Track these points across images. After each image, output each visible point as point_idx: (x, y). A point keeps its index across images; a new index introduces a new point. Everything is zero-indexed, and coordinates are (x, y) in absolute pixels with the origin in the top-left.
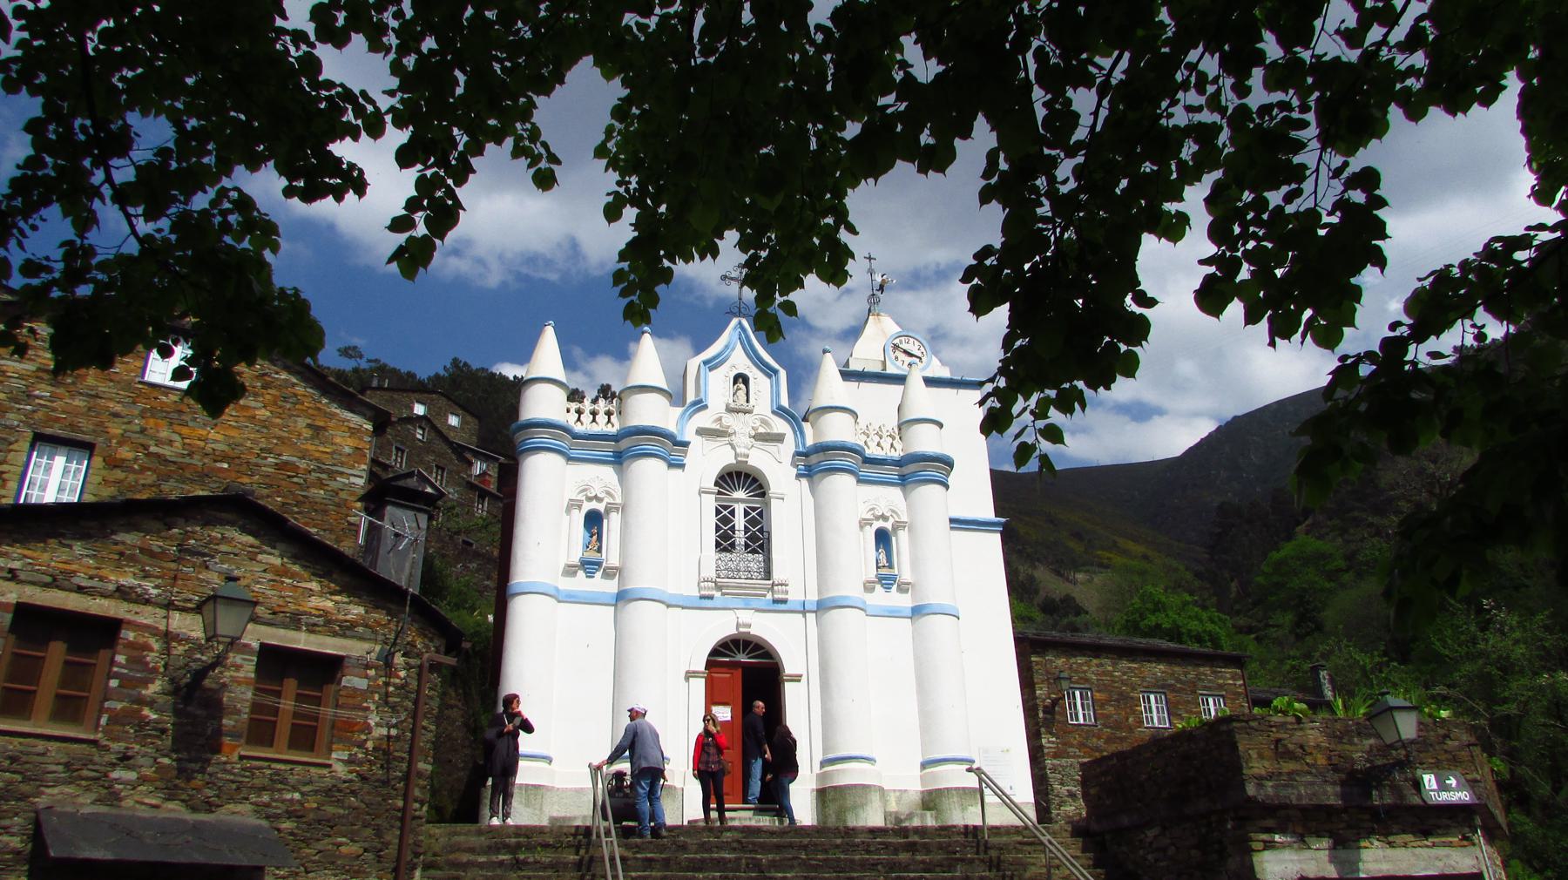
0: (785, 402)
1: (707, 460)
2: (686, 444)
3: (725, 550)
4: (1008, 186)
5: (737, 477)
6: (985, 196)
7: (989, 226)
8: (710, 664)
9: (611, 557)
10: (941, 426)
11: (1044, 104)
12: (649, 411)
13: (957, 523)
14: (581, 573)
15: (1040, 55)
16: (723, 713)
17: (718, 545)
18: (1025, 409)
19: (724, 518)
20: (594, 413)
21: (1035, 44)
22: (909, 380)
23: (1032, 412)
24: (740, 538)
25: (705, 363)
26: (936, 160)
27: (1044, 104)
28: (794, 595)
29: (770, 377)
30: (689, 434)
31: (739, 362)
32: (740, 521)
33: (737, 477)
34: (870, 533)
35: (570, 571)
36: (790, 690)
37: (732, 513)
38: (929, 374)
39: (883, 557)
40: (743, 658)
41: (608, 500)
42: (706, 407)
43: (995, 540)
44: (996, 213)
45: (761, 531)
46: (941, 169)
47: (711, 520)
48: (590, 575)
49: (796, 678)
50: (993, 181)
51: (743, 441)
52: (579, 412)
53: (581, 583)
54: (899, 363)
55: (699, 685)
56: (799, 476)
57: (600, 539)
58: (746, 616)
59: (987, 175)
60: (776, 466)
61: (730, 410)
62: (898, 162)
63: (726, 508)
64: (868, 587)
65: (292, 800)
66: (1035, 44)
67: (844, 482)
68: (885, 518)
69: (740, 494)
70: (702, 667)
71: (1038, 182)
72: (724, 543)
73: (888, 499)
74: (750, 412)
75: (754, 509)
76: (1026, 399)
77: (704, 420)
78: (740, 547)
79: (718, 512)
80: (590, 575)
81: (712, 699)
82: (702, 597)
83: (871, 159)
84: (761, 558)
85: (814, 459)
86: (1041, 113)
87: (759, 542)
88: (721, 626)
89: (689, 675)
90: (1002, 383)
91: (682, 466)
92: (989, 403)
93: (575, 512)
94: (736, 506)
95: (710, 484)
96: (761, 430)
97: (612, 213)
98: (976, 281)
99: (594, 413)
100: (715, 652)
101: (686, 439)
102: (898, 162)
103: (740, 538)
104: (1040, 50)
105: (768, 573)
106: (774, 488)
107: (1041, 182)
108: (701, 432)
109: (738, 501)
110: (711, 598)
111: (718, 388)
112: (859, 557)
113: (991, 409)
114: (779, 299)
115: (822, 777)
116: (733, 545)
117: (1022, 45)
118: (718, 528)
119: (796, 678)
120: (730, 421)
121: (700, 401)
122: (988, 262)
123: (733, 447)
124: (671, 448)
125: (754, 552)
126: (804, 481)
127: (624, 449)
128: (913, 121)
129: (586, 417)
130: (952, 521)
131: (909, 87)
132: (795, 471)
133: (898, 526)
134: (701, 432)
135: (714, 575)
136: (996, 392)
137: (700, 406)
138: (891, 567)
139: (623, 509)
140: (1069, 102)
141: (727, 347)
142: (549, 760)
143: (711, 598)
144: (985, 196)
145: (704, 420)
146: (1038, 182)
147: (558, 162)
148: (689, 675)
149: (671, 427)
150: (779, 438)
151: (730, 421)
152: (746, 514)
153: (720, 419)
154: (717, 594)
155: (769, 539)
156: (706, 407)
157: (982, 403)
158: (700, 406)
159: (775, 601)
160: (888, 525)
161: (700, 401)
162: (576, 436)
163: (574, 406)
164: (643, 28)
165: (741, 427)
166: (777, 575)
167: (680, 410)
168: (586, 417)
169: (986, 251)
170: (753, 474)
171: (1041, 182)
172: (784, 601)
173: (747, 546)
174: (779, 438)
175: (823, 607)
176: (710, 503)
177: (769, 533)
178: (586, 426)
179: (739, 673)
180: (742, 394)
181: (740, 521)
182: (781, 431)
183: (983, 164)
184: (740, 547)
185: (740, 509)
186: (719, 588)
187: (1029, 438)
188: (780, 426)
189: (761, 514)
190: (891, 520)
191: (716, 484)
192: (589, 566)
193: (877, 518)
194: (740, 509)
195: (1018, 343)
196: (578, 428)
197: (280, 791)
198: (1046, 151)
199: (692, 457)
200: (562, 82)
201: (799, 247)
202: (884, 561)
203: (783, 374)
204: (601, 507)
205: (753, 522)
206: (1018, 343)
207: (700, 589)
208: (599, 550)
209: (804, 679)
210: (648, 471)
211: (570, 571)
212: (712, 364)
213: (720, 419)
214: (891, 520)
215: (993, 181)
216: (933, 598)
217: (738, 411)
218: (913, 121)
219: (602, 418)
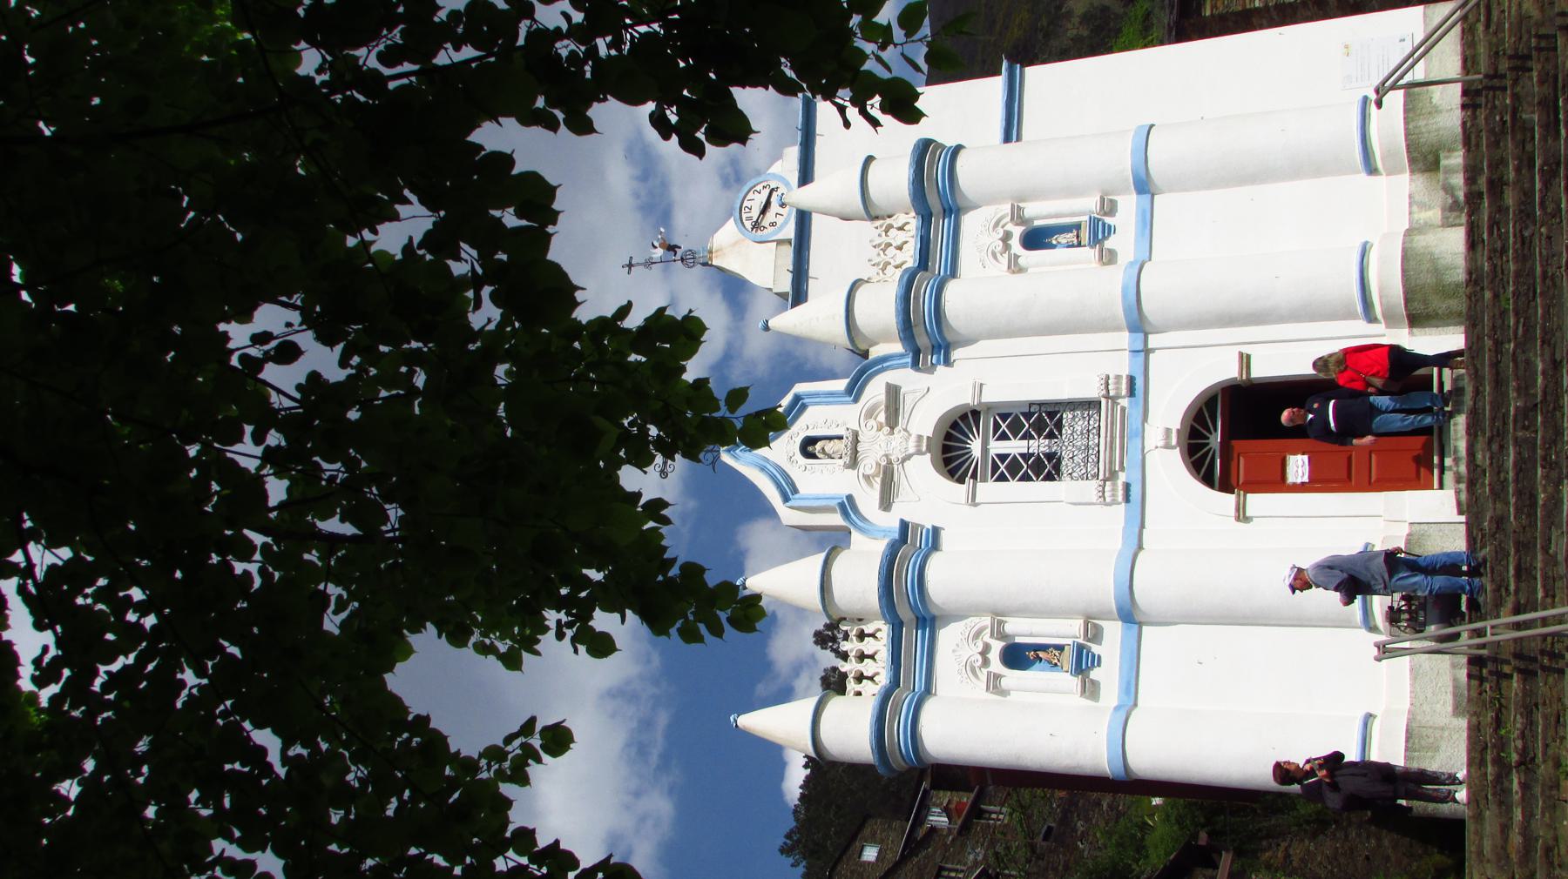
0: (840, 385)
1: (927, 495)
2: (904, 526)
3: (1057, 467)
4: (567, 97)
5: (950, 452)
6: (583, 126)
7: (622, 121)
8: (1226, 487)
9: (1068, 631)
11: (457, 49)
12: (858, 578)
13: (1011, 130)
14: (1095, 674)
15: (387, 58)
16: (1298, 467)
17: (1049, 478)
18: (879, 59)
19: (1011, 469)
20: (862, 657)
21: (373, 63)
22: (805, 205)
23: (883, 47)
24: (1039, 446)
25: (786, 499)
26: (537, 198)
27: (457, 49)
28: (1122, 366)
29: (804, 407)
30: (889, 522)
31: (782, 450)
32: (1015, 447)
33: (950, 452)
34: (1029, 257)
35: (1091, 690)
36: (1260, 371)
37: (1003, 457)
38: (794, 177)
39: (1063, 239)
40: (1216, 439)
41: (986, 637)
42: (850, 498)
43: (1037, 77)
44: (608, 113)
45: (1028, 416)
46: (550, 191)
47: (1014, 487)
48: (1096, 661)
49: (1245, 360)
50: (560, 116)
51: (897, 444)
52: (860, 678)
53: (1108, 674)
54: (780, 220)
55: (1257, 502)
56: (947, 362)
57: (1044, 648)
58: (1154, 435)
59: (552, 126)
60: (935, 395)
61: (854, 463)
62: (551, 256)
63: (995, 467)
64: (1109, 258)
66: (373, 63)
67: (956, 298)
68: (1007, 236)
69: (975, 447)
70: (1230, 499)
71: (564, 53)
72: (1046, 468)
73: (978, 233)
74: (856, 435)
75: (997, 427)
76: (863, 57)
77: (868, 501)
79: (1002, 478)
80: (1096, 661)
81: (1278, 483)
82: (1127, 499)
83: (539, 290)
84: (1067, 416)
85: (923, 341)
86: (468, 52)
87: (1044, 418)
88: (1168, 471)
90: (844, 95)
91: (936, 531)
92: (875, 112)
93: (1004, 683)
95: (961, 490)
96: (882, 417)
97: (601, 646)
98: (700, 135)
99: (862, 657)
100: (1208, 480)
101: (897, 525)
102: (551, 256)
103: (1039, 446)
104: (381, 58)
105: (1091, 405)
106: (967, 398)
107: (564, 48)
108: (886, 503)
109: (985, 450)
110: (1127, 487)
111: (822, 480)
112: (1065, 274)
113: (883, 109)
114: (723, 412)
115: (1391, 320)
116: (1050, 456)
117: (372, 82)
118: (1026, 478)
119: (1245, 360)
120: (868, 464)
121: (842, 505)
122: (674, 119)
123: (908, 457)
124: (909, 548)
125: (1059, 425)
126: (956, 354)
127: (911, 614)
128: (489, 237)
129: (868, 667)
130: (1007, 138)
131: (441, 242)
132: (941, 369)
133: (1018, 216)
134: (886, 503)
135: (1094, 485)
136: (860, 102)
137: (848, 506)
138: (1078, 226)
139: (999, 615)
140: (454, 15)
141: (763, 469)
142: (1368, 719)
143: (1127, 487)
144: (583, 126)
145: (868, 501)
146: (564, 53)
147: (532, 721)
148: (1241, 515)
149: (880, 547)
150: (893, 392)
151: (868, 464)
152: (1003, 437)
153: (867, 478)
154: (1122, 477)
155: (1041, 404)
156: (850, 498)
157: (875, 123)
158: (848, 506)
159: (1132, 392)
160: (1017, 231)
162: (895, 682)
163: (851, 685)
164: (341, 605)
166: (1092, 391)
167: (855, 535)
168: (868, 667)
169: (658, 121)
170: (946, 428)
171: (564, 48)
172: (1131, 380)
173: (1051, 436)
174: (893, 392)
175: (1138, 323)
176: (989, 489)
177: (1031, 404)
178: (880, 669)
179: (1238, 445)
180: (830, 446)
181: (1015, 447)
182: (883, 390)
183: (537, 131)
185: (997, 447)
186: (1112, 476)
187: (920, 53)
188: (875, 390)
189: (1004, 417)
190: (1010, 227)
191: (961, 481)
192: (1083, 662)
193: (1007, 247)
194: (997, 447)
195: (790, 73)
196: (884, 679)
198: (521, 42)
199: (924, 518)
200: (427, 719)
201: (665, 388)
202: (1070, 237)
203: (801, 388)
204: (997, 646)
205: (1015, 428)
206: (790, 73)
207: (1114, 502)
208: (1060, 648)
209: (1246, 350)
211: (1091, 690)
212: (788, 490)
213: (867, 478)
214: (1010, 227)
215: (560, 116)
216: (1122, 163)
217: (855, 452)
218: (489, 237)
219: (868, 646)
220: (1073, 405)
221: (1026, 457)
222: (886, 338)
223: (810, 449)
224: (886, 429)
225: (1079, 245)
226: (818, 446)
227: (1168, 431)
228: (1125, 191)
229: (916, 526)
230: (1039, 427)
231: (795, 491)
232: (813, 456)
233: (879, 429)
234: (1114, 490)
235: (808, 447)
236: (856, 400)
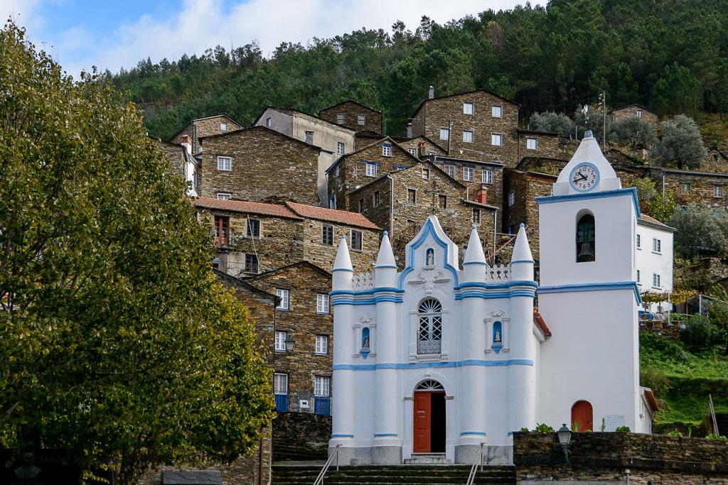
1: (413, 297)
2: (403, 291)
8: (416, 393)
14: (361, 357)
24: (430, 332)
32: (431, 325)
37: (427, 321)
40: (431, 389)
42: (413, 270)
49: (452, 398)
56: (456, 299)
57: (368, 341)
70: (411, 395)
72: (423, 335)
81: (417, 407)
85: (462, 291)
87: (438, 334)
89: (406, 399)
103: (430, 332)
116: (427, 337)
132: (454, 297)
134: (411, 283)
138: (501, 341)
152: (434, 320)
165: (430, 277)
172: (447, 363)
173: (434, 336)
174: (447, 281)
181: (431, 325)
188: (448, 275)
189: (440, 320)
192: (365, 354)
202: (498, 339)
205: (437, 324)
211: (356, 356)
220: (440, 344)
221: (427, 329)
224: (435, 280)
225: (494, 341)
227: (430, 376)
231: (415, 249)
234: (413, 360)
235: (430, 251)
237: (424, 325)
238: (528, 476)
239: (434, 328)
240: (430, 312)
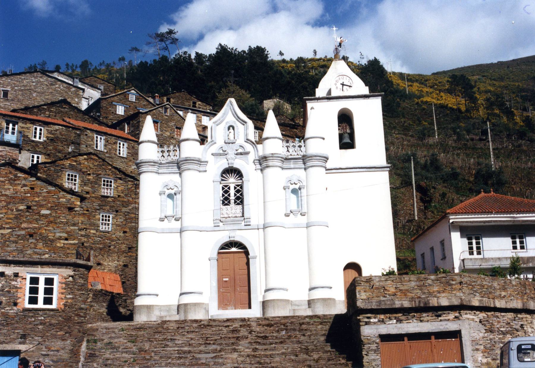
1: (216, 166)
2: (207, 162)
10: (324, 139)
17: (223, 202)
19: (226, 191)
24: (232, 198)
31: (230, 119)
32: (232, 192)
37: (229, 188)
41: (176, 189)
42: (215, 143)
45: (242, 194)
63: (226, 186)
65: (41, 320)
72: (226, 201)
75: (238, 186)
78: (232, 202)
79: (223, 189)
84: (241, 206)
87: (240, 200)
94: (230, 185)
96: (240, 150)
103: (232, 198)
118: (223, 195)
125: (238, 204)
139: (180, 192)
152: (235, 188)
161: (213, 141)
173: (235, 202)
174: (247, 153)
181: (232, 192)
184: (232, 202)
185: (232, 186)
188: (249, 147)
197: (37, 317)
199: (208, 167)
205: (238, 191)
210: (190, 175)
216: (314, 217)
221: (229, 195)
222: (263, 150)
223: (231, 128)
226: (231, 130)
228: (308, 219)
229: (206, 165)
230: (238, 198)
232: (229, 129)
233: (236, 150)
235: (231, 127)
236: (245, 142)
237: (226, 192)
238: (372, 320)
239: (235, 195)
240: (232, 181)
